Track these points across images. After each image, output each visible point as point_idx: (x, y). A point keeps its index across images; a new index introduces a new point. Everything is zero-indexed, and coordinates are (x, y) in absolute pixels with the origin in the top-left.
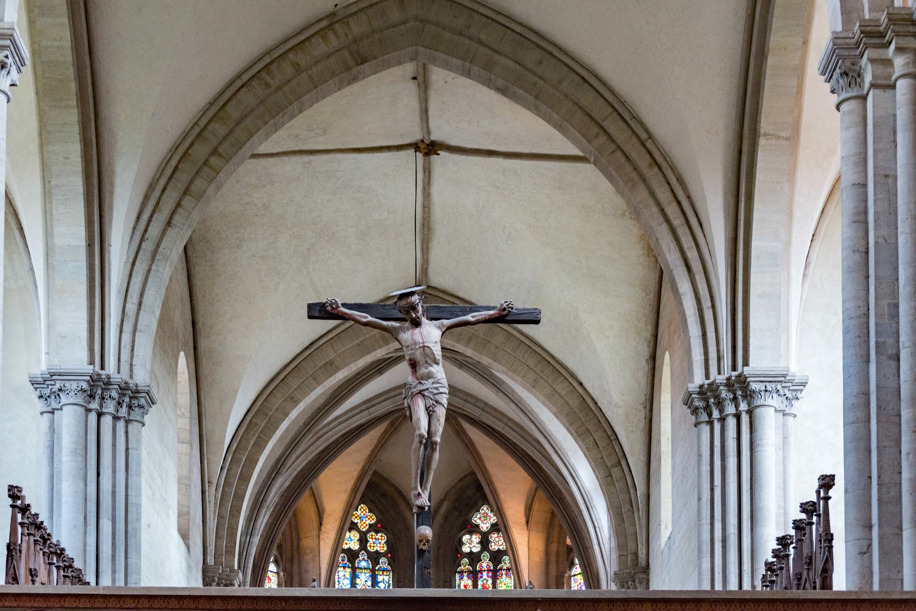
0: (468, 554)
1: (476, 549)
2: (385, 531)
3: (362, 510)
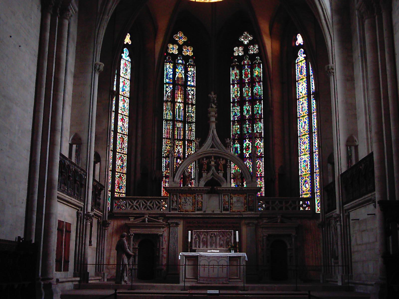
3: (180, 34)
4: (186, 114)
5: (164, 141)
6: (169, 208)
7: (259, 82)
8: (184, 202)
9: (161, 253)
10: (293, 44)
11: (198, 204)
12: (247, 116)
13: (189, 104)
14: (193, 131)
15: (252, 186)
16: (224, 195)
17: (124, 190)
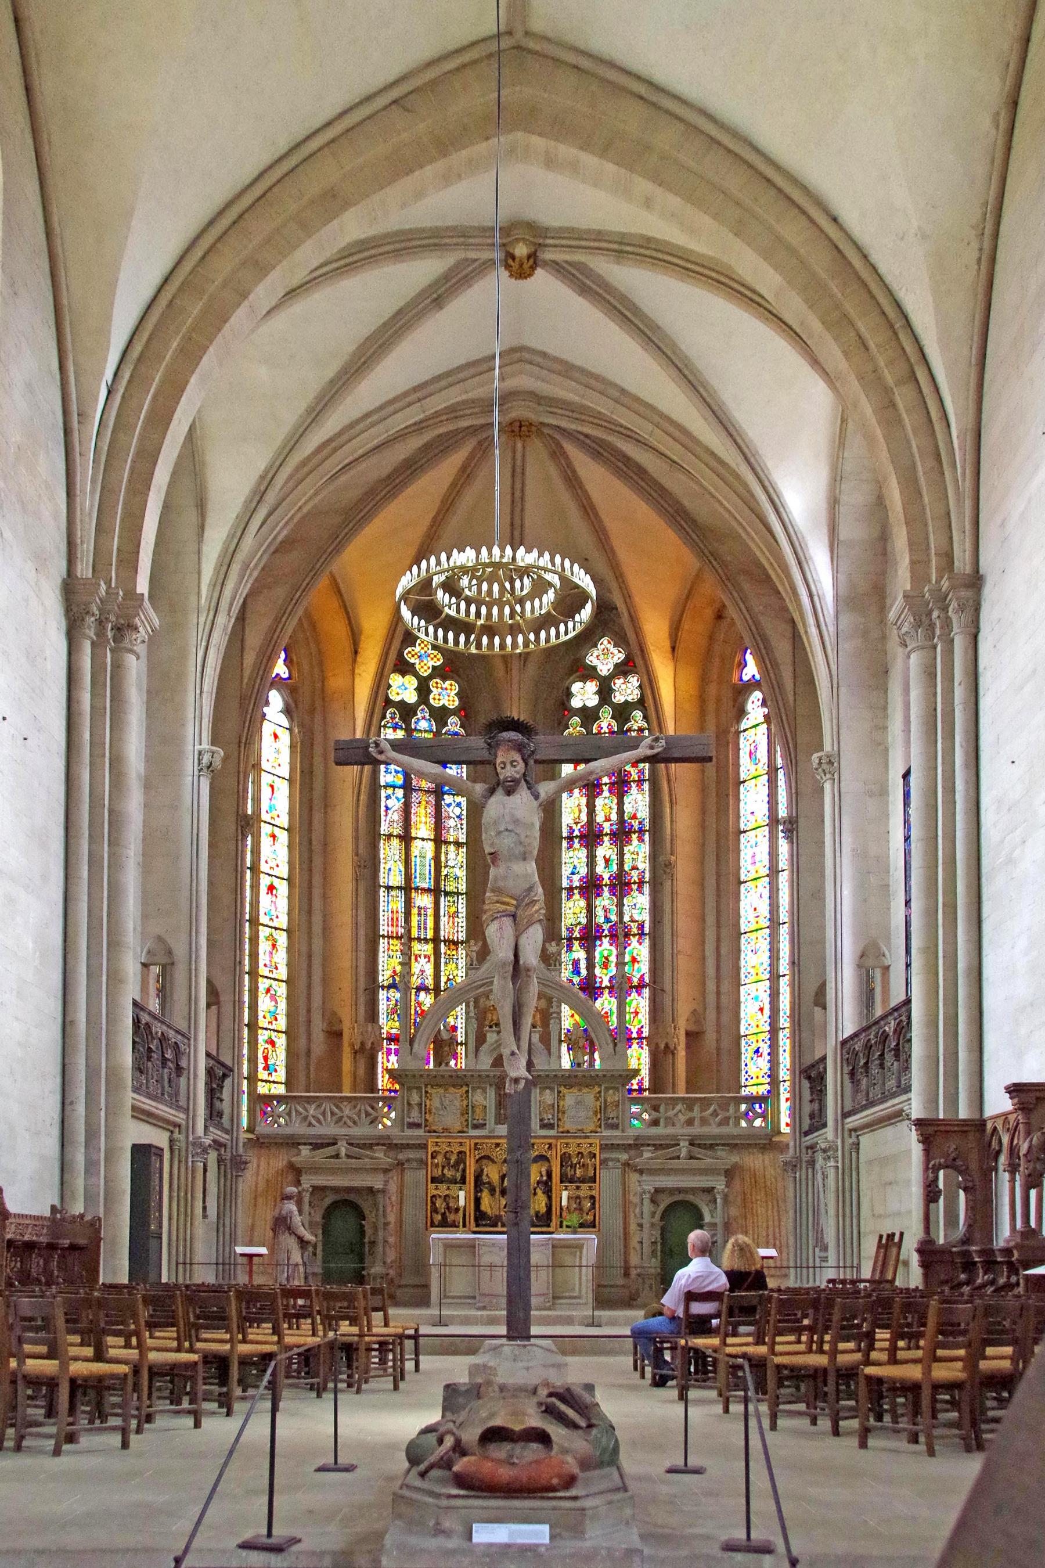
1: (593, 701)
4: (440, 872)
5: (383, 944)
6: (400, 1122)
7: (640, 782)
8: (439, 1105)
9: (381, 1233)
10: (735, 678)
11: (473, 1112)
12: (606, 876)
14: (460, 915)
16: (543, 1089)
17: (281, 1075)
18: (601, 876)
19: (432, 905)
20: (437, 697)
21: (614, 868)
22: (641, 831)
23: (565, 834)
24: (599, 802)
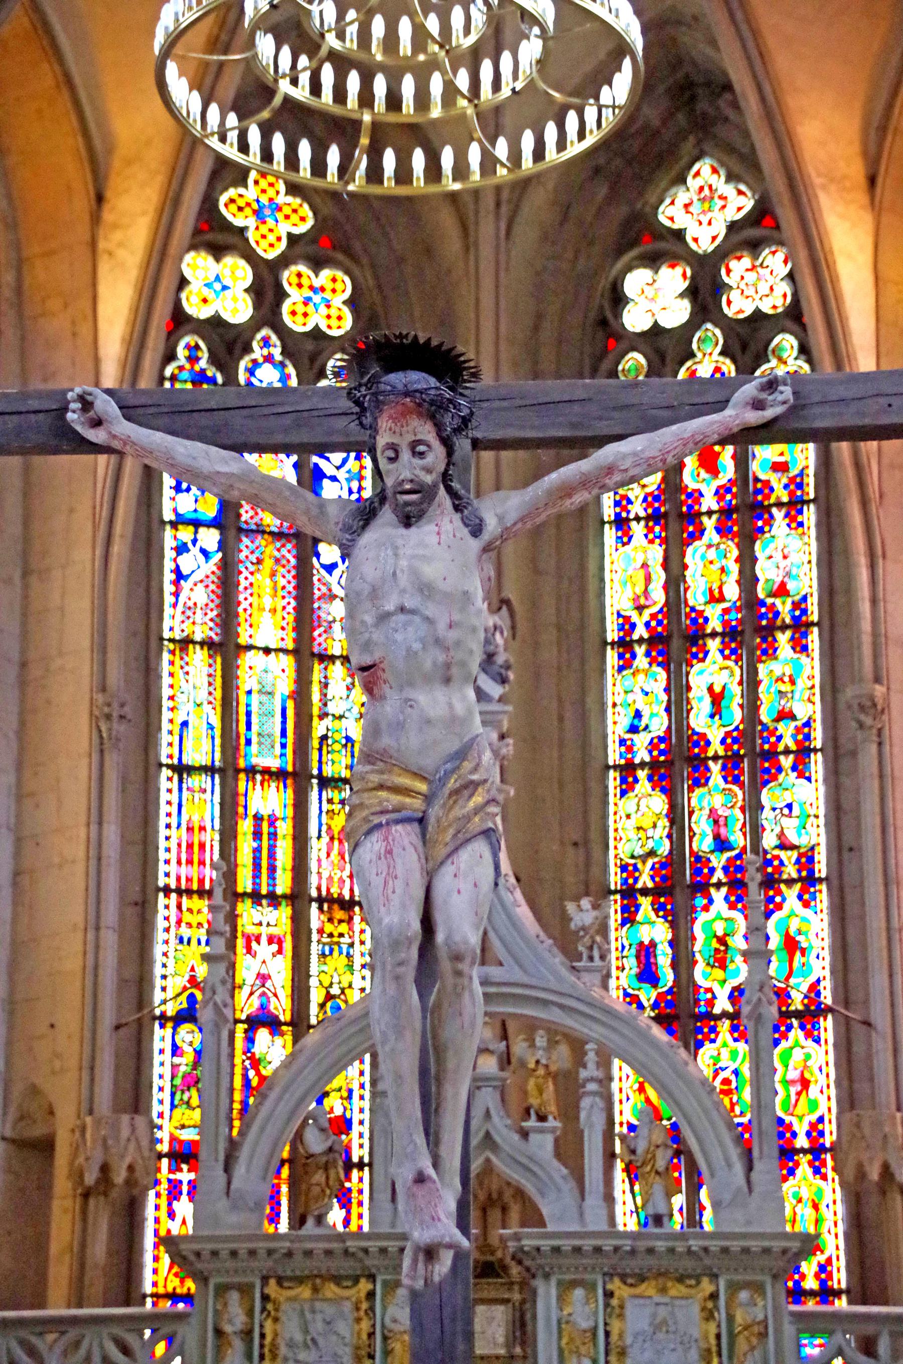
0: (643, 334)
2: (347, 262)
5: (165, 907)
7: (794, 507)
12: (715, 734)
13: (326, 658)
15: (749, 1223)
16: (566, 1287)
18: (703, 736)
19: (290, 812)
20: (300, 309)
21: (735, 714)
22: (800, 626)
23: (612, 634)
24: (694, 555)
